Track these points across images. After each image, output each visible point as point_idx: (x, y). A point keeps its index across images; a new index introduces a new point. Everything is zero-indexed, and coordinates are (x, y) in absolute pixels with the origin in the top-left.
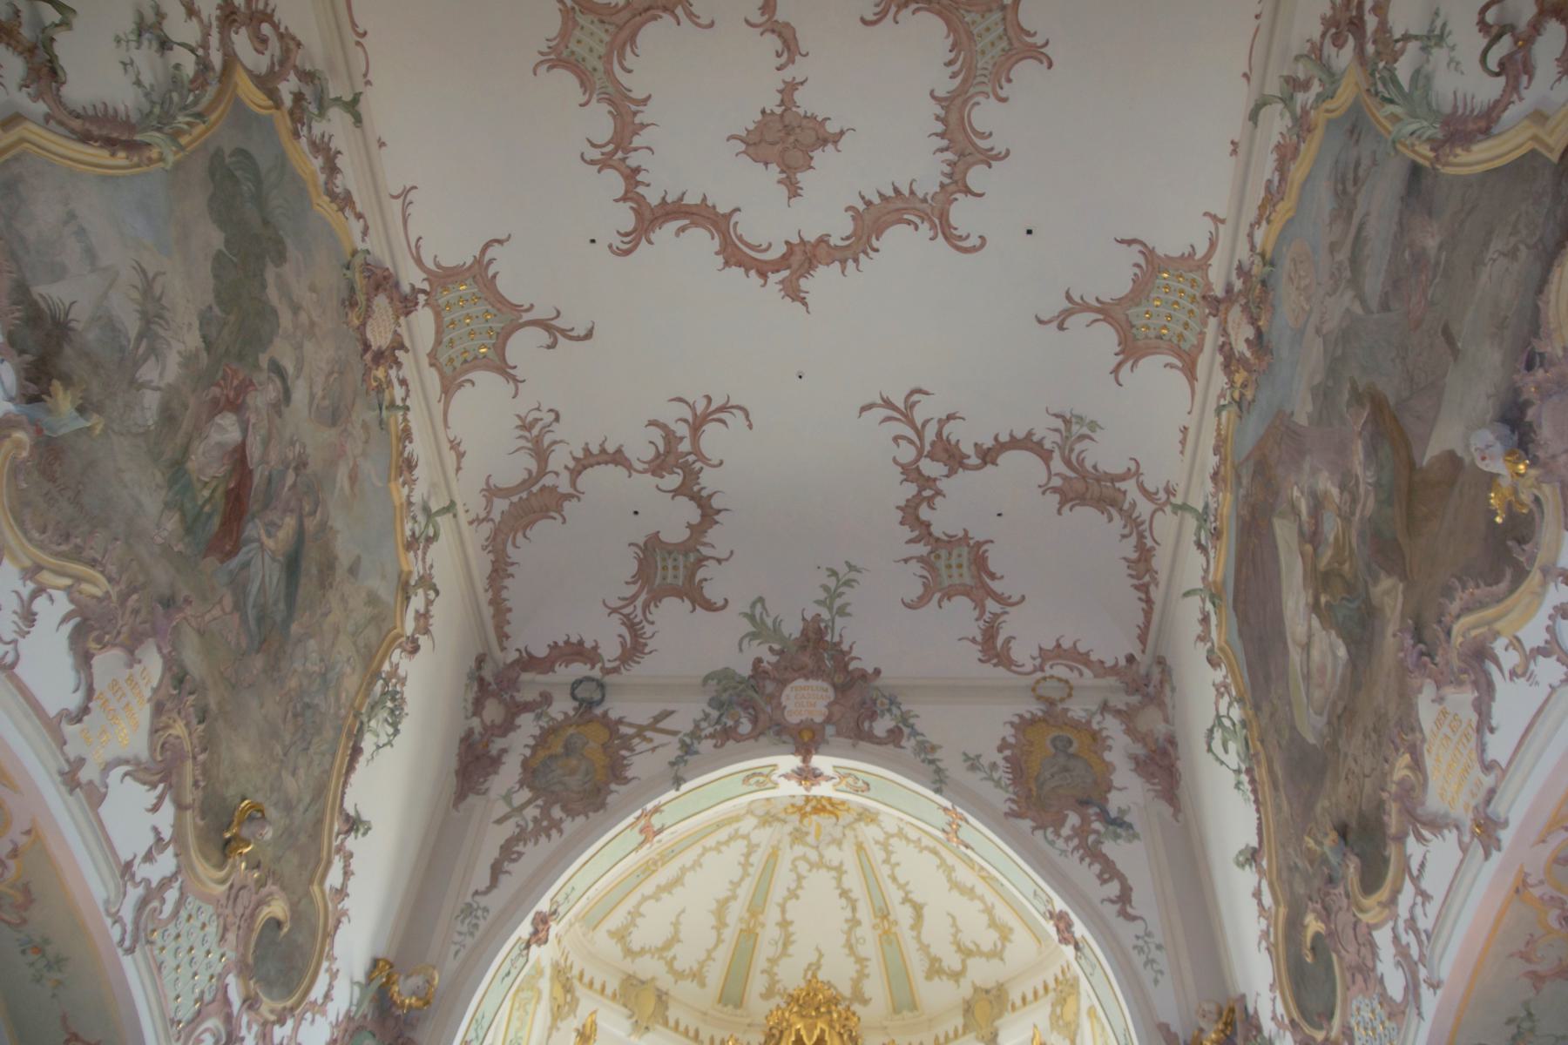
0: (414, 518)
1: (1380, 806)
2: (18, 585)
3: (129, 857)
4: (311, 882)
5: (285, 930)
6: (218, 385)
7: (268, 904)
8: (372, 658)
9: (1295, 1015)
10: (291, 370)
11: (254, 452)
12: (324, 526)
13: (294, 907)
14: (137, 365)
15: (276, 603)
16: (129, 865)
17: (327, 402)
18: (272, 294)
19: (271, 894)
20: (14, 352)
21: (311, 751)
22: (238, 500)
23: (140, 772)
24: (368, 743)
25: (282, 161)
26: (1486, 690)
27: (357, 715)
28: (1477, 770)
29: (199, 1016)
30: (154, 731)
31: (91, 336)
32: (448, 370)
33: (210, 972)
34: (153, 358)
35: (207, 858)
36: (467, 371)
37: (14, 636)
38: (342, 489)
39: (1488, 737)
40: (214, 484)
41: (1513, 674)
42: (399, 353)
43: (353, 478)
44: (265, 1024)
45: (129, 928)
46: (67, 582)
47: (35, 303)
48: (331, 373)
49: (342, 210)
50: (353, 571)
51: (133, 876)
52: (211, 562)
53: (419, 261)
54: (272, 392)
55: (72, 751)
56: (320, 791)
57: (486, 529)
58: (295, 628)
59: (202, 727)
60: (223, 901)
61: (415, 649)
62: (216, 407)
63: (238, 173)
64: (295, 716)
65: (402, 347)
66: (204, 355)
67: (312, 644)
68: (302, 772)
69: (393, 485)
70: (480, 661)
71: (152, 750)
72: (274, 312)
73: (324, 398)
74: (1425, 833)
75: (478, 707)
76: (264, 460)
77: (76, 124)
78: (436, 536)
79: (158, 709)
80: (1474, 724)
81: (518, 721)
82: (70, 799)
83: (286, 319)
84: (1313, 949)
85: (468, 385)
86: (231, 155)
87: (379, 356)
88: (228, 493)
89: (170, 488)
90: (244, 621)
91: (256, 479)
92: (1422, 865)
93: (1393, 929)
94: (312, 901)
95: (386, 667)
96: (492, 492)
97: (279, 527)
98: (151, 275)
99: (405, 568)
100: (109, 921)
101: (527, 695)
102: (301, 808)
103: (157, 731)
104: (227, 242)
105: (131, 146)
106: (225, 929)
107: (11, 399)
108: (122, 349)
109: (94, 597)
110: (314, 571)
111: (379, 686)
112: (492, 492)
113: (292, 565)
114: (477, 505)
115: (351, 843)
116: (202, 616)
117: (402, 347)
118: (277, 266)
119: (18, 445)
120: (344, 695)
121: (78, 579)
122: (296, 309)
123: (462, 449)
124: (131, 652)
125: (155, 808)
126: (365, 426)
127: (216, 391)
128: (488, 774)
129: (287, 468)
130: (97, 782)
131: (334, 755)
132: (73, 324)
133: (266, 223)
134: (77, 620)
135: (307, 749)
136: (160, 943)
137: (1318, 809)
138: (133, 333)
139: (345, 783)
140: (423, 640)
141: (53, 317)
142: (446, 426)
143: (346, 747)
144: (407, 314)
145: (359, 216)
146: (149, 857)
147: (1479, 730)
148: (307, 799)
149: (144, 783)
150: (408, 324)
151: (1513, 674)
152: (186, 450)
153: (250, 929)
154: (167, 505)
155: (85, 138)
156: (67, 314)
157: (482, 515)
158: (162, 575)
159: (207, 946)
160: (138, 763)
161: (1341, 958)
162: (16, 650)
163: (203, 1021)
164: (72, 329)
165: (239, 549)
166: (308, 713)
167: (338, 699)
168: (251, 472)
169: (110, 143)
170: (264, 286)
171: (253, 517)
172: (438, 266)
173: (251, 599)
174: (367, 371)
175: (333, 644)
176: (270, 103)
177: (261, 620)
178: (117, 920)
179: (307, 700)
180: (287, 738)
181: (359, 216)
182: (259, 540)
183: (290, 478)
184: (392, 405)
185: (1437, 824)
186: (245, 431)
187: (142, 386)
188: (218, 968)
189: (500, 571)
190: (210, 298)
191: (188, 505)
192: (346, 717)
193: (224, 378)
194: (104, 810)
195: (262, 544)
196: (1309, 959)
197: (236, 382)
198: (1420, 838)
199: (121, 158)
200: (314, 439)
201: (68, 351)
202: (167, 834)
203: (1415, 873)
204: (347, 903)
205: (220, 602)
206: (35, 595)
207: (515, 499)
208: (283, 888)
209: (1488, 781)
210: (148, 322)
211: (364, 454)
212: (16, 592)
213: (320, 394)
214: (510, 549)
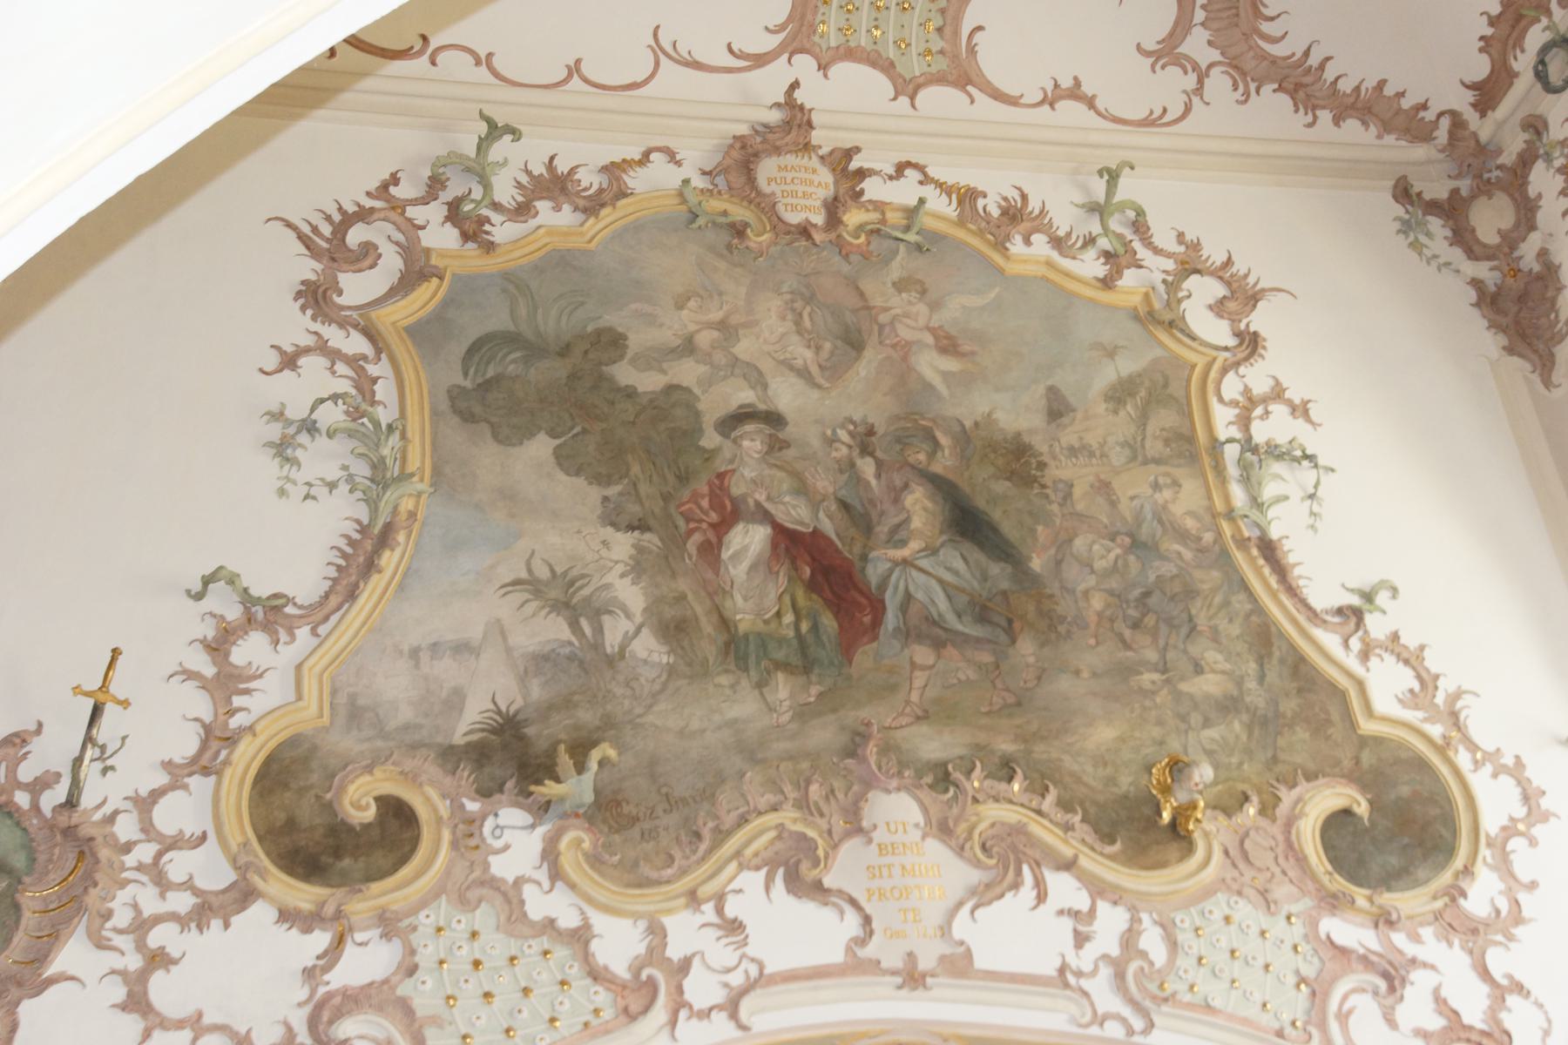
0: (1090, 241)
2: (699, 919)
3: (1058, 963)
4: (1352, 725)
5: (1362, 809)
6: (690, 533)
7: (1302, 814)
8: (1191, 439)
10: (743, 396)
11: (796, 513)
12: (964, 438)
13: (1357, 777)
14: (597, 646)
15: (985, 578)
16: (1062, 971)
17: (828, 346)
18: (648, 382)
19: (1298, 800)
20: (497, 797)
21: (1202, 622)
22: (829, 574)
23: (984, 895)
24: (1283, 524)
25: (513, 283)
27: (1230, 515)
29: (1318, 993)
30: (960, 850)
31: (537, 691)
32: (940, 64)
33: (1288, 946)
34: (606, 619)
35: (1162, 865)
36: (956, 33)
37: (739, 952)
38: (945, 375)
40: (787, 599)
42: (855, 164)
43: (948, 345)
44: (1438, 916)
45: (1127, 1012)
46: (733, 866)
47: (468, 744)
48: (798, 323)
49: (623, 194)
50: (1057, 409)
51: (1079, 974)
52: (864, 657)
53: (760, 60)
54: (752, 442)
55: (893, 960)
56: (1264, 637)
57: (1218, 82)
58: (1036, 564)
59: (1016, 787)
60: (1231, 873)
61: (1251, 343)
62: (711, 551)
63: (490, 373)
64: (1136, 625)
65: (849, 153)
66: (648, 536)
67: (1079, 544)
68: (1212, 656)
69: (1012, 268)
70: (1403, 192)
71: (977, 864)
72: (671, 389)
73: (818, 349)
75: (1463, 237)
76: (815, 507)
77: (334, 601)
78: (1140, 213)
79: (944, 830)
81: (1532, 192)
82: (935, 992)
83: (687, 373)
85: (978, 37)
86: (466, 374)
87: (833, 209)
88: (812, 586)
89: (746, 670)
90: (962, 640)
91: (828, 527)
94: (1379, 741)
95: (1224, 421)
96: (1166, 53)
97: (907, 520)
98: (524, 575)
99: (1136, 300)
100: (1094, 1030)
101: (1514, 145)
102: (1251, 684)
103: (962, 848)
104: (553, 434)
105: (384, 539)
106: (1264, 893)
107: (533, 826)
108: (571, 658)
109: (772, 842)
110: (1001, 487)
111: (1231, 452)
112: (1166, 53)
113: (967, 522)
114: (1176, 82)
115: (1376, 625)
116: (908, 702)
117: (849, 153)
118: (622, 357)
119: (579, 842)
120: (1190, 523)
121: (738, 854)
122: (688, 347)
123: (1066, 83)
124: (860, 830)
125: (1041, 897)
126: (900, 286)
127: (692, 545)
128: (1553, 301)
129: (852, 465)
130: (948, 950)
131: (1245, 586)
132: (512, 710)
133: (565, 351)
134: (781, 871)
135: (1193, 629)
136: (1181, 987)
138: (565, 633)
139: (1292, 591)
140: (1258, 320)
141: (493, 731)
142: (1012, 101)
143: (1252, 560)
144: (810, 125)
145: (645, 159)
146: (1080, 940)
148: (1252, 667)
149: (1002, 896)
150: (823, 127)
152: (725, 623)
153: (1301, 860)
154: (760, 685)
155: (352, 595)
156: (499, 712)
157: (1191, 81)
158: (824, 735)
159: (1254, 931)
160: (973, 892)
162: (753, 960)
163: (1327, 994)
164: (517, 713)
165: (882, 602)
166: (1153, 601)
167: (1183, 536)
168: (816, 533)
169: (370, 567)
170: (630, 393)
171: (864, 558)
172: (781, 28)
173: (952, 620)
174: (839, 245)
175: (1113, 504)
176: (435, 281)
177: (982, 613)
178: (1100, 1020)
179: (1136, 593)
180: (1152, 655)
181: (645, 159)
182: (896, 563)
183: (867, 467)
184: (912, 213)
186: (766, 517)
187: (623, 648)
188: (1298, 929)
189: (1303, 84)
190: (594, 493)
191: (780, 655)
192: (1219, 535)
193: (688, 520)
194: (980, 963)
195: (906, 563)
197: (705, 503)
199: (388, 559)
200: (861, 395)
201: (530, 731)
202: (1082, 901)
204: (1446, 686)
205: (913, 665)
206: (720, 910)
207: (1200, 15)
208: (1310, 777)
210: (567, 605)
211: (935, 306)
212: (704, 925)
213: (809, 354)
214: (1277, 50)
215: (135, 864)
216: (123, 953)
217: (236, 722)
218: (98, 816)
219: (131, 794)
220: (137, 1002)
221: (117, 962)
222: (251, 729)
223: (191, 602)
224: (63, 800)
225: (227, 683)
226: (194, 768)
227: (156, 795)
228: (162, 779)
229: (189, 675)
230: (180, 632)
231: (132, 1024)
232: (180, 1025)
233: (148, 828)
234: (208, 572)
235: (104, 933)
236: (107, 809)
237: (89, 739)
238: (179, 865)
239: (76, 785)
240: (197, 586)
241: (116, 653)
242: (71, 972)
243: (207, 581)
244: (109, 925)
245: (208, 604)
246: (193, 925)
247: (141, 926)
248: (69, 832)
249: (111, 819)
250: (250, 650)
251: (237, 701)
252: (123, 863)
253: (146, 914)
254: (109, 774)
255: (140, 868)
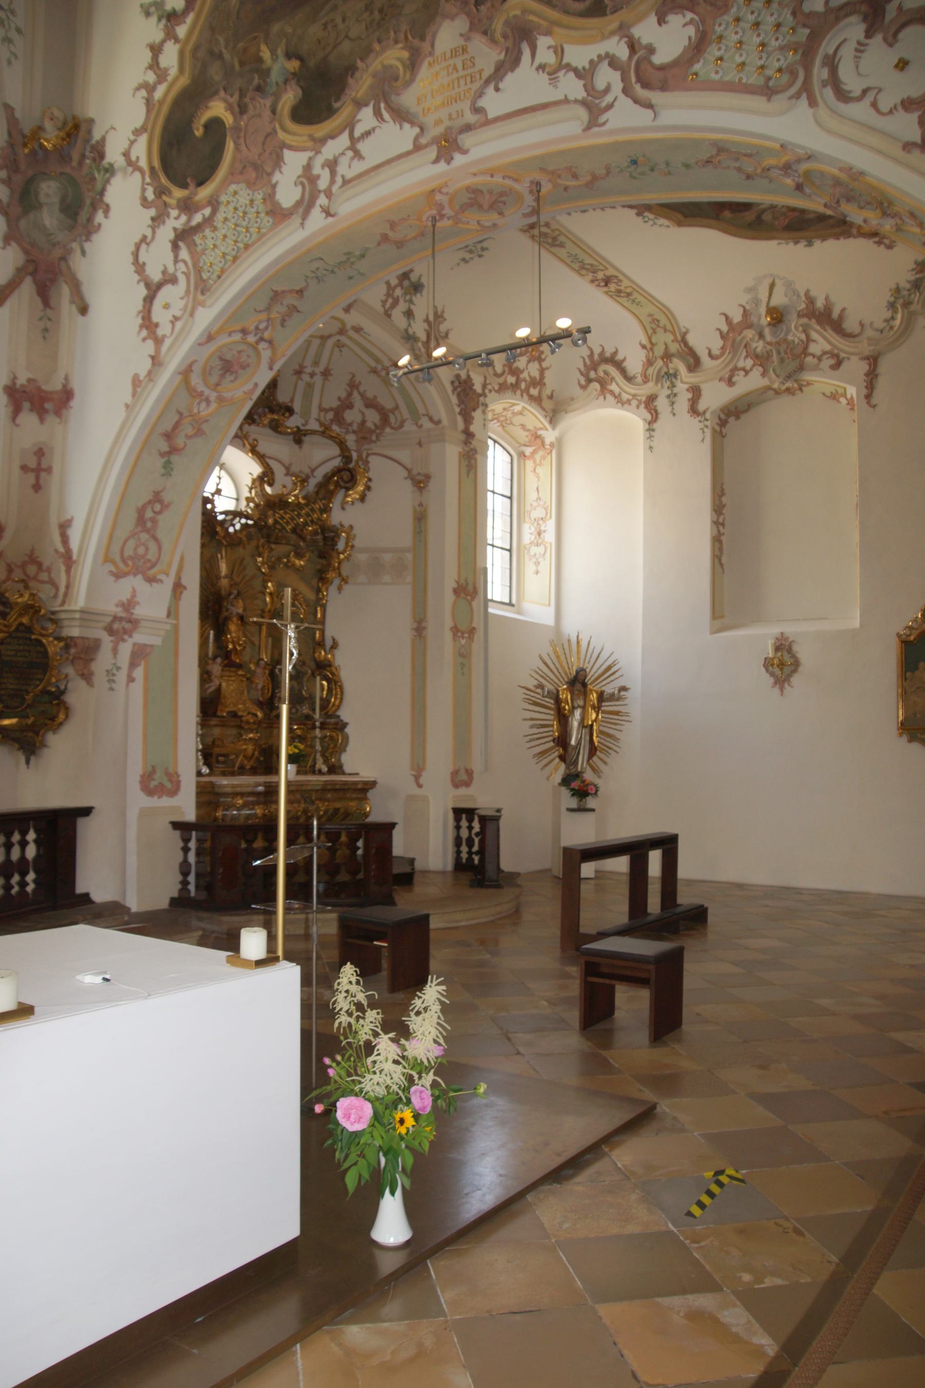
1: (351, 69)
9: (156, 164)
26: (511, 62)
28: (466, 106)
39: (490, 89)
41: (542, 67)
74: (386, 116)
80: (486, 75)
84: (207, 126)
92: (368, 134)
93: (310, 159)
137: (276, 28)
147: (487, 82)
151: (542, 67)
161: (237, 148)
185: (401, 116)
196: (199, 132)
198: (377, 114)
203: (357, 134)
209: (470, 118)
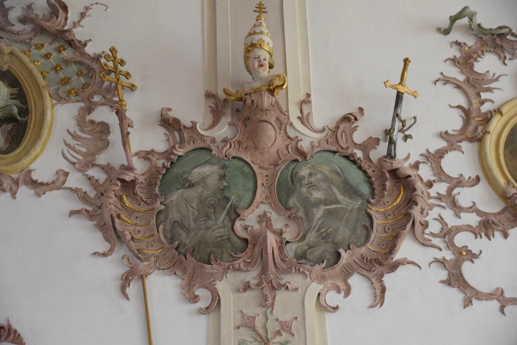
215: (436, 195)
216: (441, 250)
217: (485, 108)
218: (406, 164)
219: (424, 152)
220: (456, 279)
221: (439, 255)
222: (499, 111)
223: (442, 36)
224: (386, 154)
225: (475, 85)
226: (463, 136)
227: (440, 154)
228: (442, 144)
229: (447, 81)
230: (436, 56)
231: (455, 295)
232: (489, 296)
233: (441, 175)
234: (454, 13)
235: (425, 236)
236: (412, 161)
237: (396, 115)
238: (465, 196)
239: (392, 142)
240: (446, 23)
241: (406, 61)
242: (410, 259)
243: (453, 20)
244: (427, 231)
245: (454, 36)
246: (483, 234)
247: (448, 234)
248: (394, 173)
249: (416, 166)
250: (487, 64)
251: (484, 96)
252: (429, 194)
253: (450, 226)
254: (408, 140)
255: (439, 197)
